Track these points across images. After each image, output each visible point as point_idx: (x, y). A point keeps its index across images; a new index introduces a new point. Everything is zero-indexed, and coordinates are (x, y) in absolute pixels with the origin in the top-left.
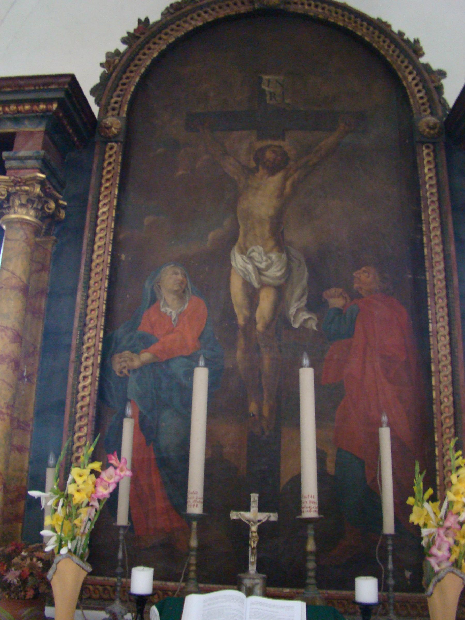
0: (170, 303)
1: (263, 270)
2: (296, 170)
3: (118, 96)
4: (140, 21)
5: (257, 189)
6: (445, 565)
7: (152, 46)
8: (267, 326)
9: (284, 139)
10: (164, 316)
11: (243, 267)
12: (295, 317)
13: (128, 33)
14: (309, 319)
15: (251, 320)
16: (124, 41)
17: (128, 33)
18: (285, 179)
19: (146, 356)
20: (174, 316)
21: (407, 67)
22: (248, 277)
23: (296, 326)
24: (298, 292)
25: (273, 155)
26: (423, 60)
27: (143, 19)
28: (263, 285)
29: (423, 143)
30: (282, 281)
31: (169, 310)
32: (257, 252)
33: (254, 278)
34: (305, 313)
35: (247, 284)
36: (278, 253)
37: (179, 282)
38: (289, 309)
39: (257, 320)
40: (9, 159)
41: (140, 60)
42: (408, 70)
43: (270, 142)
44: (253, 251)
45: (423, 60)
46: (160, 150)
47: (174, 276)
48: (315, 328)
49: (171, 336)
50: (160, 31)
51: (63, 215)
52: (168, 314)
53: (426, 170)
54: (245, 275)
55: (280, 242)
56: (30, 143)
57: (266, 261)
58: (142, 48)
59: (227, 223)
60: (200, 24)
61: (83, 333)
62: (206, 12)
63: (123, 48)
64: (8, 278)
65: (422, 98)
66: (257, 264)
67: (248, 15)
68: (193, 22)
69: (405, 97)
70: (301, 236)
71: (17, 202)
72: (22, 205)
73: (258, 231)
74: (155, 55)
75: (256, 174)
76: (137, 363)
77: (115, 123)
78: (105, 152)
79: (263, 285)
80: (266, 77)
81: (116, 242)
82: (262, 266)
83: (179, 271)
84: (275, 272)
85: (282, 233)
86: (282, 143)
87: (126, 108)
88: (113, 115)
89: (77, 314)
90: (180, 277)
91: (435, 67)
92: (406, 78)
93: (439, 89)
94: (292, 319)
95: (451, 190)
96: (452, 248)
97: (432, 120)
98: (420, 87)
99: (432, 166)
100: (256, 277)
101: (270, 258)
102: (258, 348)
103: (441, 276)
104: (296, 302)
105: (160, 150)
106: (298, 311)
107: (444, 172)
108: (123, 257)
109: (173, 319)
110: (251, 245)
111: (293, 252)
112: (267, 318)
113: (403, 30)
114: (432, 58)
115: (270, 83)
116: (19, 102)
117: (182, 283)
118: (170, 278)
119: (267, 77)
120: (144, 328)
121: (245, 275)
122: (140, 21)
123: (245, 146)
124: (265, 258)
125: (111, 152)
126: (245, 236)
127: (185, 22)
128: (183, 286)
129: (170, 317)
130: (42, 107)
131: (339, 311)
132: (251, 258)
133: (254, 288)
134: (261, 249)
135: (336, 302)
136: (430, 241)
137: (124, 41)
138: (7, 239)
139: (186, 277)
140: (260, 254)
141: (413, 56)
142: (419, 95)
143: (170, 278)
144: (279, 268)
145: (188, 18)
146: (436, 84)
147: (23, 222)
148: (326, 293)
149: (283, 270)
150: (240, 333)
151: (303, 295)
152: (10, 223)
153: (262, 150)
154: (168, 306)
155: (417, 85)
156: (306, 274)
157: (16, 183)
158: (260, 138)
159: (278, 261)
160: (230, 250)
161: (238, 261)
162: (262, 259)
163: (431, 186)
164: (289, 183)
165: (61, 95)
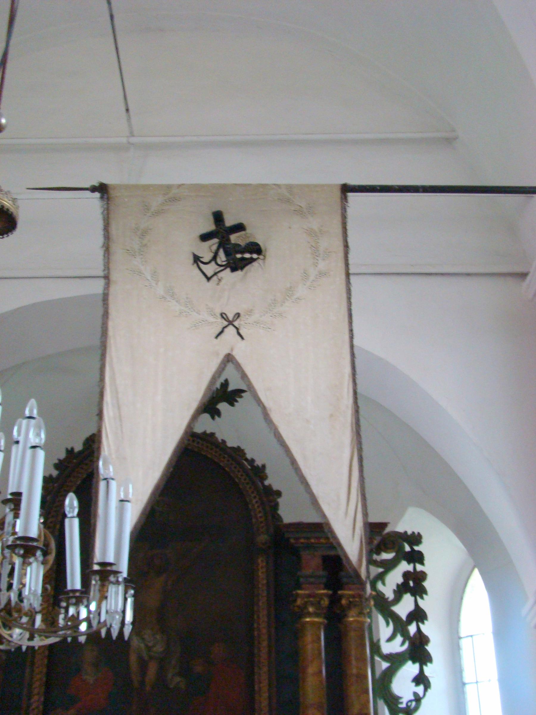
4: (67, 449)
15: (142, 683)
20: (92, 682)
24: (173, 662)
26: (266, 483)
42: (253, 495)
45: (266, 483)
65: (261, 517)
79: (151, 658)
82: (150, 644)
84: (159, 648)
91: (275, 487)
106: (173, 676)
113: (255, 458)
122: (67, 449)
132: (143, 639)
135: (199, 669)
146: (273, 504)
155: (258, 507)
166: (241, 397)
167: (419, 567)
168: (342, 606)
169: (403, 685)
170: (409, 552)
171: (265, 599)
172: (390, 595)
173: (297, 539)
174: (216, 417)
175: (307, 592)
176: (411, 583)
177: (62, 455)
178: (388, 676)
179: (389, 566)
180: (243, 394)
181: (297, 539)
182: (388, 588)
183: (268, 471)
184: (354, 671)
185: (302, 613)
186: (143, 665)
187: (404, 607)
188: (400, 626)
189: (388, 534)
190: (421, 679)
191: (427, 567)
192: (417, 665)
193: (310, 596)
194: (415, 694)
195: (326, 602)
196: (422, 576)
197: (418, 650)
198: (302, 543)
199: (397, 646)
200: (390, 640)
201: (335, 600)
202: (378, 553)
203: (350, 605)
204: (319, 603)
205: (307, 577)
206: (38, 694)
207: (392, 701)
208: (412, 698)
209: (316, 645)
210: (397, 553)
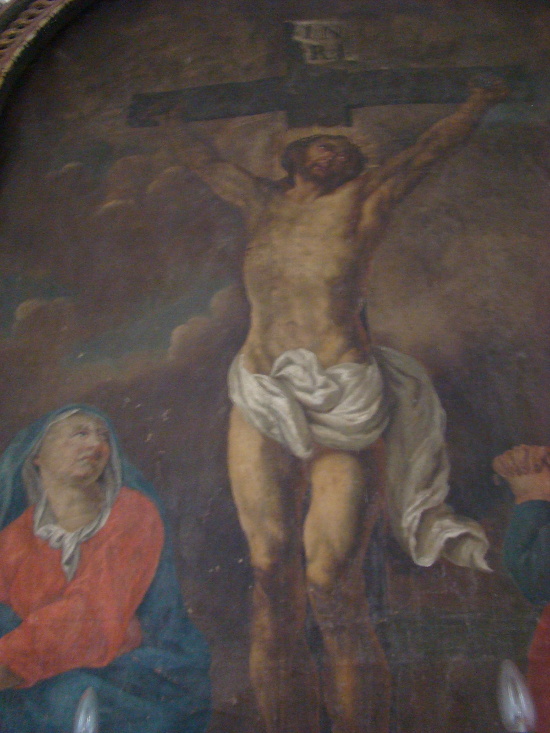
0: (60, 511)
1: (319, 409)
2: (384, 179)
5: (293, 221)
8: (339, 569)
9: (349, 123)
11: (263, 405)
12: (420, 533)
14: (463, 537)
15: (291, 552)
18: (360, 198)
20: (69, 549)
22: (275, 431)
24: (421, 463)
25: (326, 154)
30: (375, 434)
31: (57, 531)
32: (300, 364)
33: (294, 430)
34: (447, 522)
35: (274, 450)
36: (357, 367)
37: (89, 453)
38: (400, 516)
39: (308, 551)
43: (317, 131)
44: (289, 362)
46: (71, 165)
47: (77, 439)
48: (484, 566)
49: (56, 609)
52: (53, 542)
54: (269, 426)
55: (361, 341)
57: (325, 386)
59: (219, 300)
66: (301, 395)
73: (298, 315)
75: (290, 192)
79: (321, 450)
82: (316, 399)
83: (91, 425)
84: (352, 414)
85: (363, 316)
86: (343, 131)
90: (92, 441)
94: (412, 542)
100: (298, 427)
101: (335, 378)
102: (316, 636)
104: (417, 491)
105: (71, 165)
109: (66, 557)
110: (283, 348)
111: (399, 360)
112: (337, 545)
117: (98, 455)
119: (305, 23)
121: (269, 426)
123: (261, 140)
124: (321, 379)
126: (266, 327)
128: (101, 464)
129: (60, 550)
132: (283, 381)
133: (296, 461)
134: (309, 356)
139: (108, 440)
140: (305, 369)
143: (69, 443)
144: (360, 404)
148: (501, 463)
149: (374, 408)
150: (258, 593)
151: (435, 472)
153: (302, 145)
154: (56, 521)
156: (439, 414)
158: (292, 124)
159: (356, 386)
160: (228, 362)
161: (249, 390)
162: (314, 381)
164: (369, 206)
186: (291, 483)
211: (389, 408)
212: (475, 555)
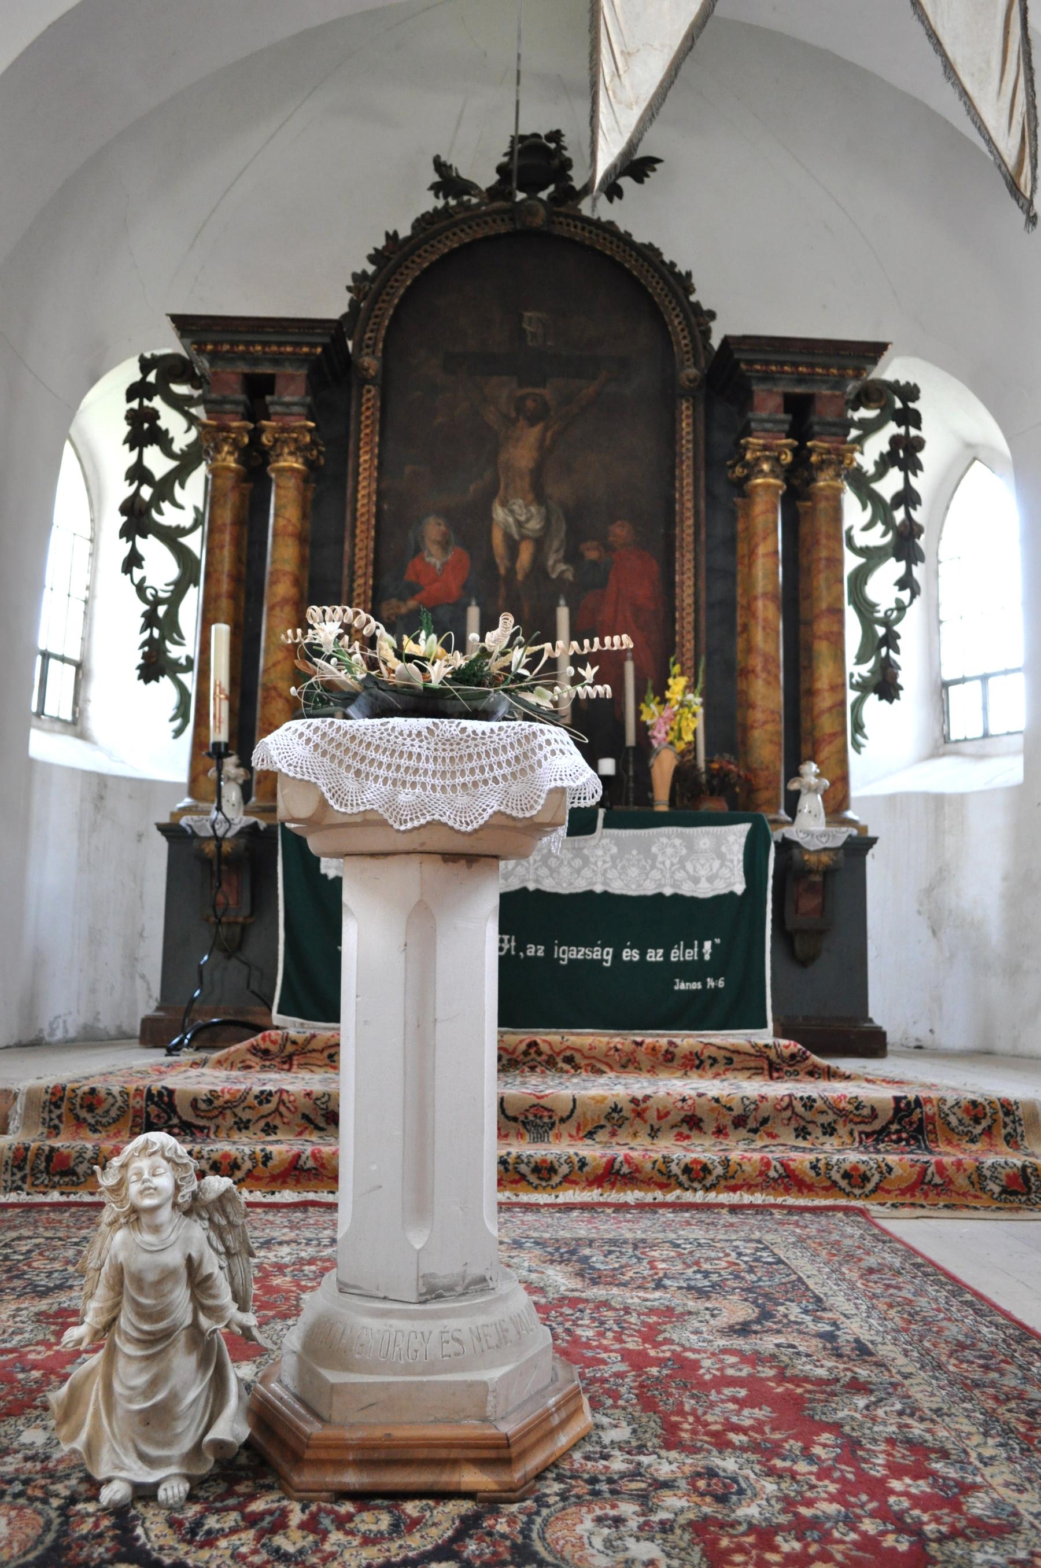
3: (372, 331)
4: (387, 234)
6: (664, 744)
7: (406, 272)
8: (527, 576)
10: (428, 565)
13: (376, 249)
15: (512, 571)
16: (372, 259)
17: (376, 249)
19: (412, 604)
20: (438, 565)
21: (674, 309)
23: (554, 576)
24: (556, 544)
26: (693, 298)
27: (391, 233)
28: (524, 537)
29: (682, 396)
32: (518, 504)
40: (273, 403)
41: (392, 287)
45: (693, 298)
50: (412, 252)
51: (322, 461)
53: (684, 425)
55: (539, 496)
56: (292, 388)
58: (394, 273)
60: (456, 245)
61: (352, 581)
62: (462, 230)
63: (371, 269)
64: (285, 526)
67: (507, 235)
68: (448, 243)
69: (670, 343)
70: (559, 490)
71: (286, 450)
72: (291, 453)
74: (408, 283)
76: (404, 610)
77: (371, 363)
78: (362, 396)
79: (524, 537)
80: (527, 314)
81: (379, 493)
82: (523, 518)
84: (535, 525)
87: (381, 346)
88: (367, 354)
89: (346, 562)
90: (443, 528)
91: (705, 307)
92: (672, 321)
93: (707, 333)
95: (707, 444)
96: (702, 505)
97: (692, 372)
98: (686, 333)
99: (690, 421)
103: (691, 531)
106: (556, 562)
107: (701, 428)
108: (386, 507)
114: (703, 296)
115: (532, 320)
116: (280, 344)
118: (433, 529)
120: (409, 576)
122: (387, 234)
125: (369, 396)
126: (507, 487)
127: (439, 242)
130: (305, 349)
131: (594, 564)
132: (512, 512)
133: (514, 541)
135: (592, 555)
136: (682, 495)
137: (372, 259)
138: (278, 487)
141: (681, 292)
142: (683, 342)
143: (433, 529)
145: (443, 237)
147: (292, 470)
148: (582, 547)
152: (280, 471)
153: (523, 398)
155: (682, 330)
156: (564, 527)
157: (283, 430)
161: (499, 514)
163: (688, 441)
164: (549, 434)
165: (327, 340)
166: (654, 170)
167: (913, 432)
168: (811, 465)
169: (882, 587)
170: (899, 410)
171: (690, 462)
172: (870, 468)
173: (750, 363)
174: (616, 199)
175: (761, 442)
176: (901, 454)
177: (381, 243)
178: (860, 577)
179: (870, 428)
180: (657, 166)
181: (750, 363)
182: (867, 458)
183: (695, 280)
184: (824, 553)
185: (753, 470)
186: (513, 547)
187: (890, 485)
188: (882, 510)
189: (873, 381)
190: (906, 582)
191: (928, 431)
192: (903, 564)
193: (765, 447)
194: (898, 601)
195: (787, 458)
196: (919, 444)
197: (906, 544)
198: (757, 371)
199: (876, 537)
200: (866, 528)
201: (801, 454)
202: (856, 409)
203: (822, 465)
204: (777, 459)
205: (763, 421)
206: (365, 574)
207: (865, 609)
208: (893, 605)
209: (770, 516)
210: (882, 409)
211: (547, 521)
212: (569, 576)
